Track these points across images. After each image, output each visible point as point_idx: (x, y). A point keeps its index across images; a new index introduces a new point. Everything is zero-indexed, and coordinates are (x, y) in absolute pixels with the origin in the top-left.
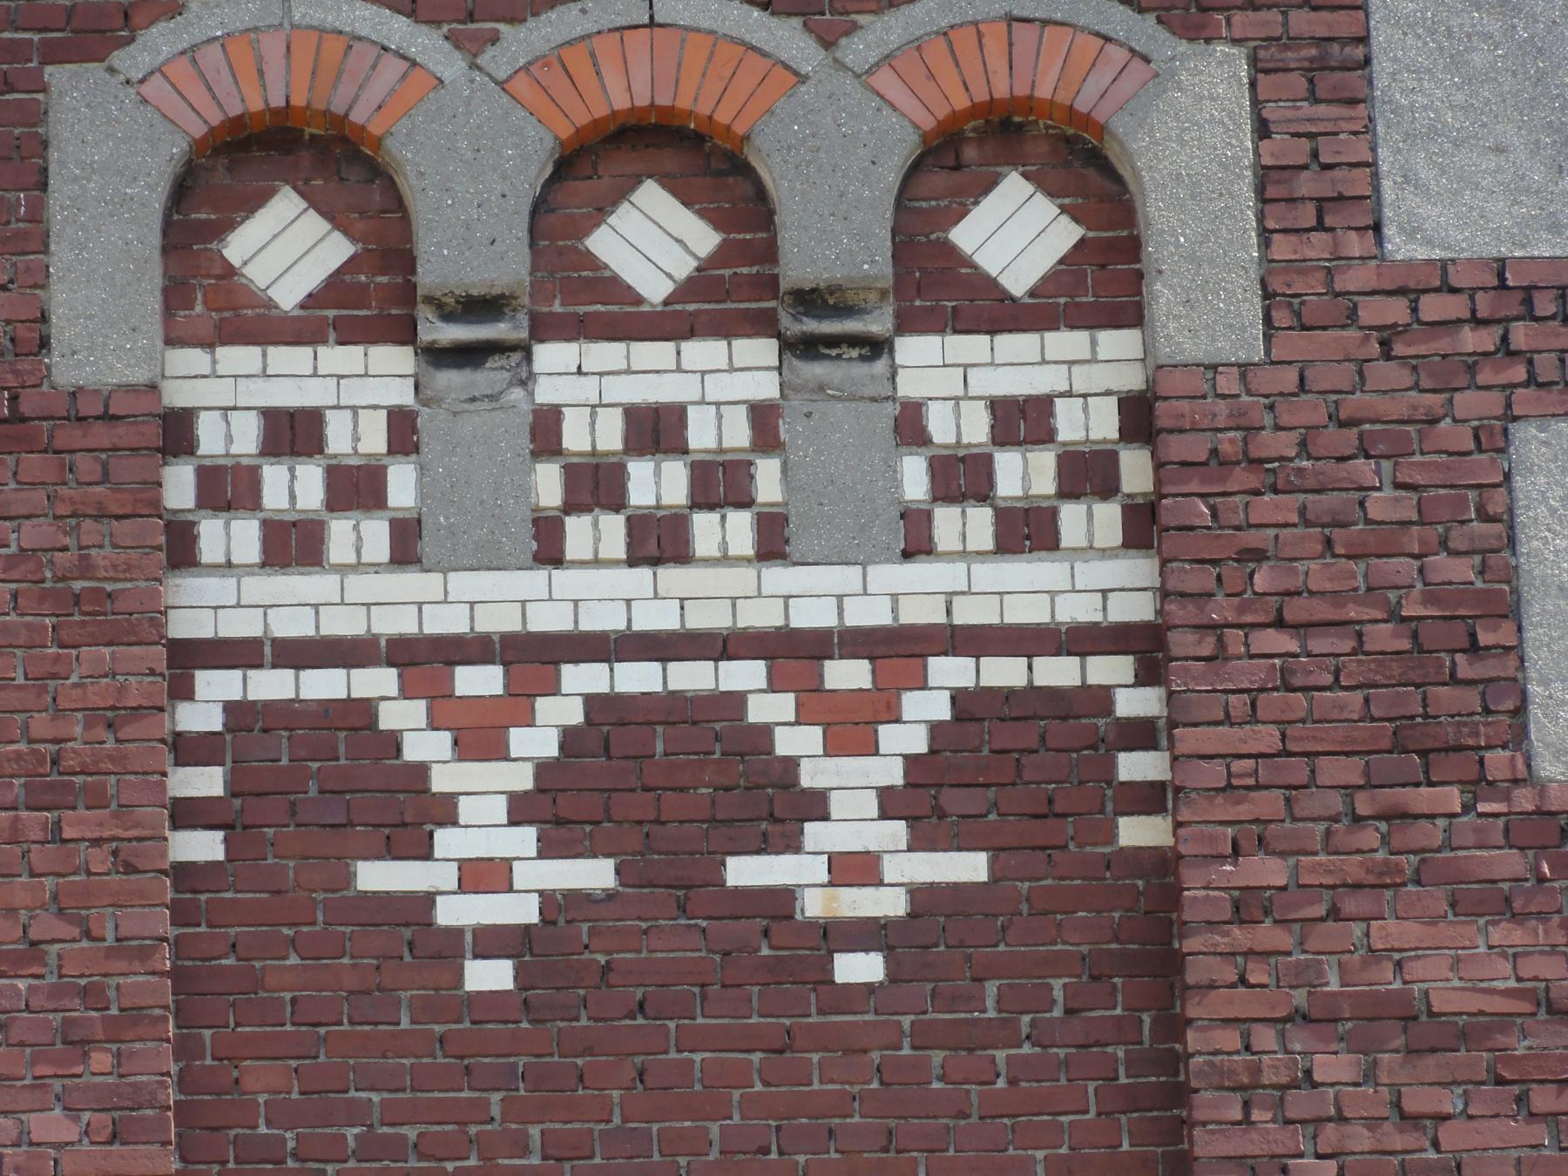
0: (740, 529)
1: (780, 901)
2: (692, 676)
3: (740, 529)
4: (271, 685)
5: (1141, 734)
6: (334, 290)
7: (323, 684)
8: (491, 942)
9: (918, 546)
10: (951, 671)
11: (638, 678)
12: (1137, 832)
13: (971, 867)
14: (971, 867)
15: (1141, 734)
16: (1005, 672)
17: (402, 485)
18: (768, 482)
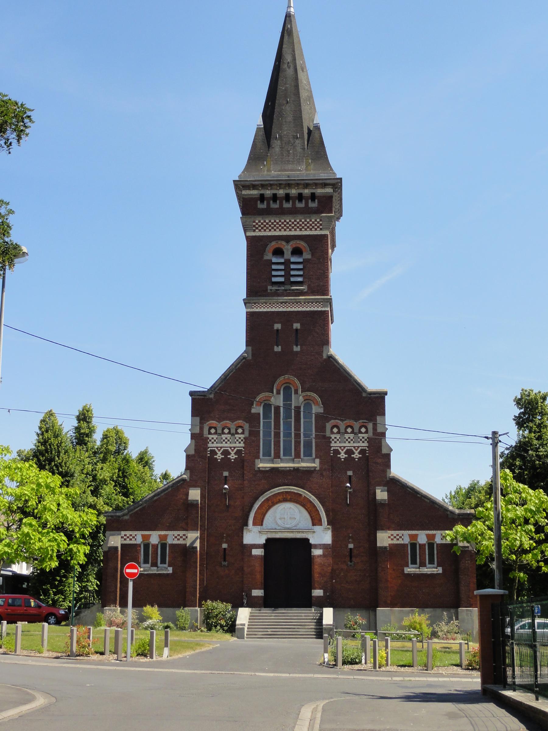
0: (352, 442)
1: (353, 457)
2: (350, 448)
3: (352, 442)
4: (335, 448)
5: (367, 450)
6: (337, 432)
7: (337, 448)
8: (343, 458)
9: (359, 442)
10: (360, 448)
11: (348, 448)
12: (367, 454)
13: (361, 456)
14: (361, 456)
15: (367, 450)
16: (362, 448)
17: (340, 440)
18: (354, 440)
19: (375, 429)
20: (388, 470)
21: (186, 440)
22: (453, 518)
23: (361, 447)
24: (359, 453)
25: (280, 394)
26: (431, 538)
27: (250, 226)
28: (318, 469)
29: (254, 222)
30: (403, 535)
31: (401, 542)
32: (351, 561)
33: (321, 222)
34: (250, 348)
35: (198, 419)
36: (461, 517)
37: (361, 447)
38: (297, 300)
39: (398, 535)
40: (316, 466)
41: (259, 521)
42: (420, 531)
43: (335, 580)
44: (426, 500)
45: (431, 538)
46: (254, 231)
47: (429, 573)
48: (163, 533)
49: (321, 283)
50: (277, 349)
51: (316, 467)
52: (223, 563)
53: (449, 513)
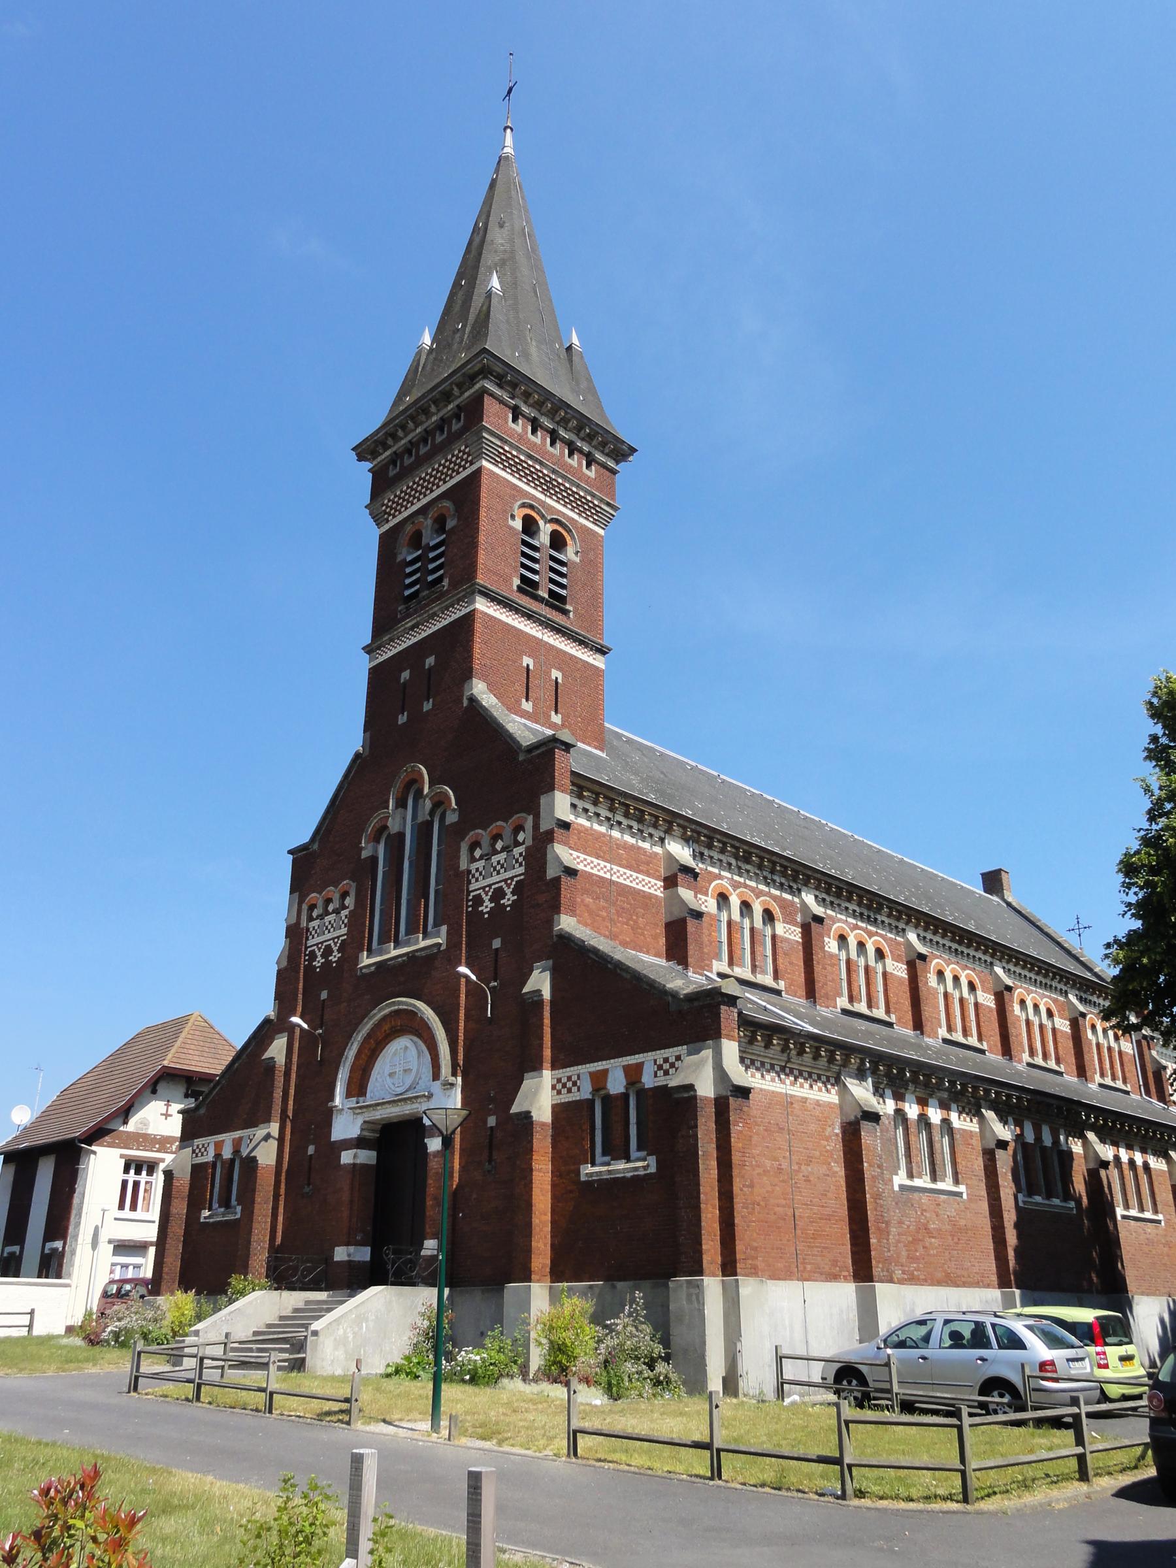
19: (536, 826)
20: (556, 916)
21: (278, 943)
22: (680, 1012)
23: (516, 876)
24: (513, 893)
25: (404, 806)
26: (633, 1074)
27: (380, 516)
28: (443, 948)
29: (383, 505)
30: (579, 1078)
31: (575, 1096)
32: (490, 1162)
33: (467, 450)
34: (368, 734)
35: (296, 895)
36: (696, 1004)
37: (516, 876)
38: (431, 612)
39: (569, 1078)
40: (441, 942)
41: (358, 1087)
42: (612, 1061)
43: (462, 1212)
44: (624, 974)
45: (633, 1074)
46: (388, 521)
47: (629, 1175)
48: (237, 1134)
49: (468, 562)
50: (402, 719)
51: (440, 945)
52: (307, 1189)
53: (670, 998)
